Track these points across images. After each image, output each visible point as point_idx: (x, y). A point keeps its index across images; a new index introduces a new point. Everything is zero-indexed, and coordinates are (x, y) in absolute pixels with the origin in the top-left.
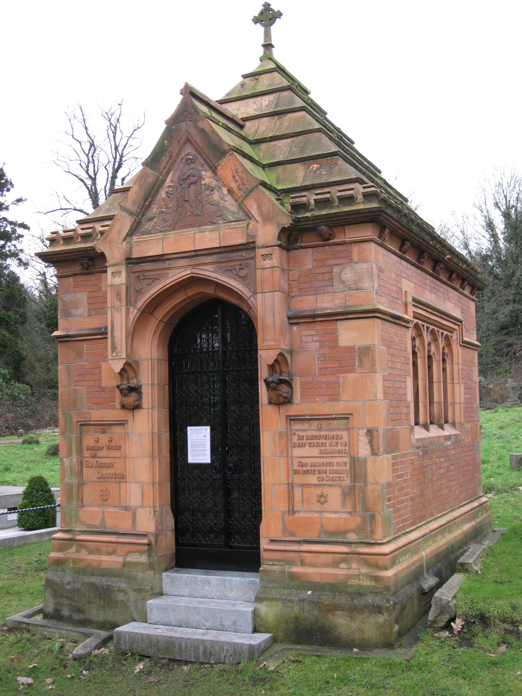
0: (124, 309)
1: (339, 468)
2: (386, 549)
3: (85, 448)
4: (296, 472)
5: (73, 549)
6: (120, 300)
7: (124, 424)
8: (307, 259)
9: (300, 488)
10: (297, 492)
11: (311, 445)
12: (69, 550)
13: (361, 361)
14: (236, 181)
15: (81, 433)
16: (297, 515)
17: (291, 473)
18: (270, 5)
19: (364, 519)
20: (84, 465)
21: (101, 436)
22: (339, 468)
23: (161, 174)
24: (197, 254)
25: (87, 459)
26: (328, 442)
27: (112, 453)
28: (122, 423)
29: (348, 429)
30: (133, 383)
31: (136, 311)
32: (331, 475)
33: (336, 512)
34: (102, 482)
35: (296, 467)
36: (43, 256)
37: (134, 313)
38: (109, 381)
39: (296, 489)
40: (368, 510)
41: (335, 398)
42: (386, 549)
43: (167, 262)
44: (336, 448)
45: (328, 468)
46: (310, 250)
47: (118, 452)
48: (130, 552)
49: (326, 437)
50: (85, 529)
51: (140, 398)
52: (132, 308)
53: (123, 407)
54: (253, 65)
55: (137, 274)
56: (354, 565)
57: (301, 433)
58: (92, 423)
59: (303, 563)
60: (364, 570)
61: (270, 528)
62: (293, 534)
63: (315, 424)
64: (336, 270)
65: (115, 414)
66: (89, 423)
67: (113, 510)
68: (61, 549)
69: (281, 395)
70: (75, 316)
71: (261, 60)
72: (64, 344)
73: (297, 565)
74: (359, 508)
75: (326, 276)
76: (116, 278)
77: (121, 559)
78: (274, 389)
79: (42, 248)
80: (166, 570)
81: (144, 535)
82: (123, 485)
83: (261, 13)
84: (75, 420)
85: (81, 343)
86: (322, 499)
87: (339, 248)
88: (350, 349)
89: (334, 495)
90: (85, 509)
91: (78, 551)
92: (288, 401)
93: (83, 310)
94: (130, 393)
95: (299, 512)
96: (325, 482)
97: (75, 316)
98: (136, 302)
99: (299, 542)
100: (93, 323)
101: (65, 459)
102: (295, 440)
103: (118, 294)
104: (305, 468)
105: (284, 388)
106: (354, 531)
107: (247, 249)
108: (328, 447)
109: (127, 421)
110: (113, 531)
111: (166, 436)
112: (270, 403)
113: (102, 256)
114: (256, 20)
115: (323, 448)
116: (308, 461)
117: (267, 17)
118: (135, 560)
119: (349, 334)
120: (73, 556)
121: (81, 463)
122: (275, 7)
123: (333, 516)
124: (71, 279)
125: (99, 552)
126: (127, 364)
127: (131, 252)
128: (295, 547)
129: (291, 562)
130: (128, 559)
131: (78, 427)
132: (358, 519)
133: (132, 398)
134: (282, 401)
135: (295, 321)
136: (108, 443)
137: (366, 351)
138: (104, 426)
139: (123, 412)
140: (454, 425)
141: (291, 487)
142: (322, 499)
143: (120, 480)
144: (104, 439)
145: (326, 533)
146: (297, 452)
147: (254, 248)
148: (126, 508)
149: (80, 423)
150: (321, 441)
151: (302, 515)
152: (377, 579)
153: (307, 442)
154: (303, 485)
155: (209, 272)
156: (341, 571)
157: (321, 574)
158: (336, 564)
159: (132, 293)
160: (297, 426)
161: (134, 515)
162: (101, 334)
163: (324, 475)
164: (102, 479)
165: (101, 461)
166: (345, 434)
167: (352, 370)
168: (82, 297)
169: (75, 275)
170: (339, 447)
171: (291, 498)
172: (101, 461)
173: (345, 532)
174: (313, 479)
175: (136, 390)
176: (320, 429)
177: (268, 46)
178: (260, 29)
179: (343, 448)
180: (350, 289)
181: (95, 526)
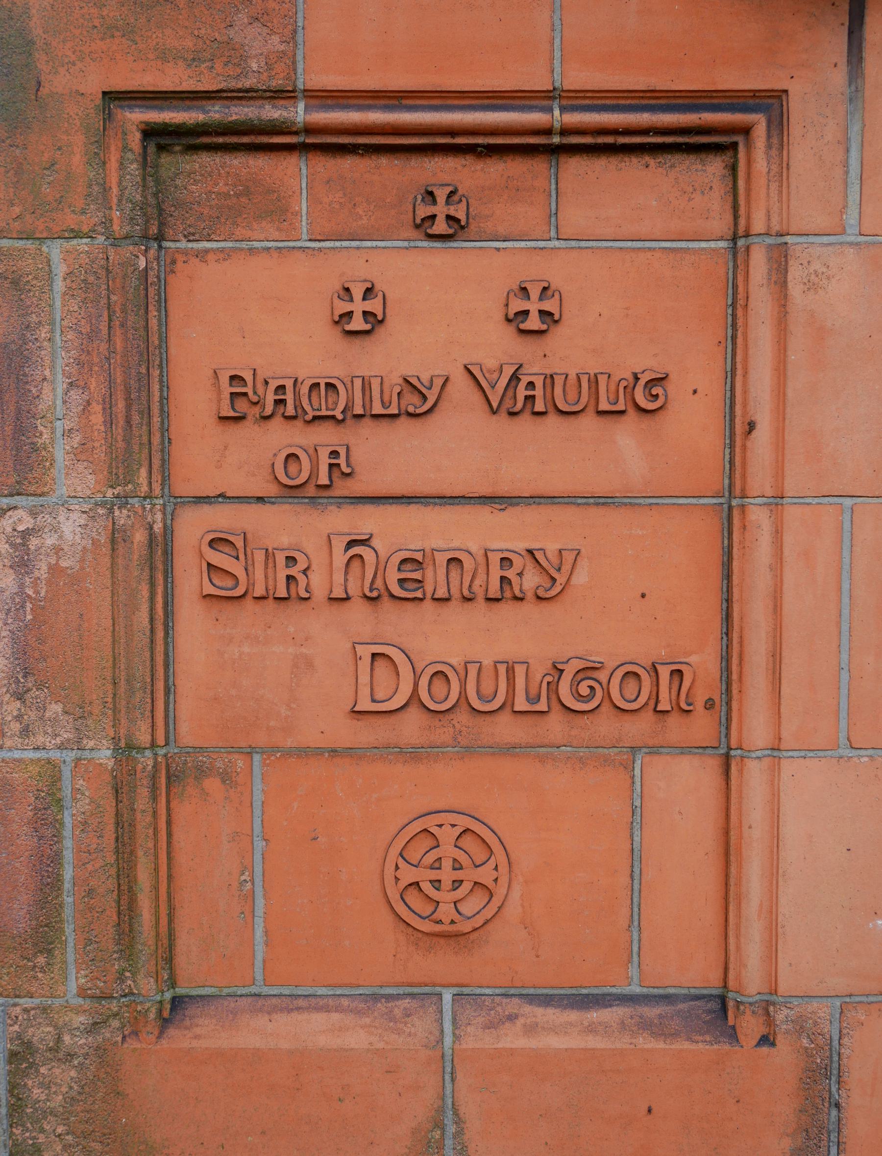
3: (195, 401)
20: (189, 581)
21: (406, 270)
25: (222, 518)
34: (413, 755)
47: (627, 440)
58: (300, 113)
66: (271, 112)
67: (562, 1034)
84: (78, 77)
90: (203, 1034)
109: (772, 103)
121: (161, 550)
131: (123, 171)
136: (496, 348)
143: (638, 728)
144: (445, 309)
149: (136, 117)
165: (395, 532)
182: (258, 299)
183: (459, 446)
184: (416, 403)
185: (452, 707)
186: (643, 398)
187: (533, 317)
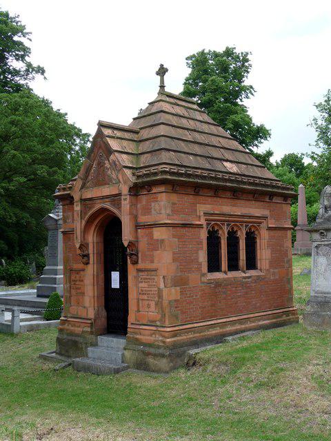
2: (168, 329)
19: (162, 317)
37: (84, 222)
41: (152, 262)
42: (168, 329)
49: (149, 279)
51: (89, 260)
54: (154, 96)
61: (131, 318)
62: (138, 321)
63: (146, 273)
65: (81, 266)
80: (101, 335)
83: (159, 70)
88: (158, 240)
89: (153, 304)
111: (102, 276)
119: (158, 234)
122: (165, 66)
125: (74, 326)
128: (138, 327)
129: (136, 333)
134: (135, 263)
137: (163, 241)
140: (261, 270)
141: (138, 300)
142: (149, 306)
145: (149, 321)
146: (141, 285)
152: (164, 342)
154: (142, 300)
155: (108, 206)
156: (152, 339)
158: (151, 335)
159: (83, 213)
160: (140, 274)
161: (87, 310)
171: (138, 305)
175: (87, 256)
177: (162, 87)
178: (159, 77)
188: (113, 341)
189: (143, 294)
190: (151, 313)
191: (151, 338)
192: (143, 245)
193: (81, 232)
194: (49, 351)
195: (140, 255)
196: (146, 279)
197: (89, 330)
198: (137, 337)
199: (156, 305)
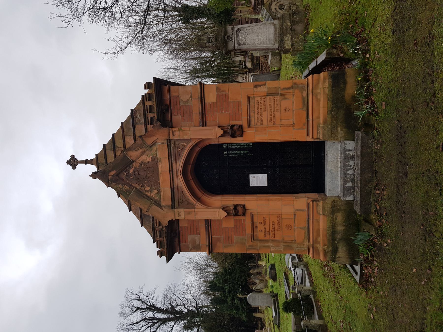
0: (196, 210)
1: (272, 101)
3: (265, 238)
4: (274, 123)
5: (318, 246)
6: (192, 212)
7: (253, 215)
8: (177, 118)
9: (282, 121)
10: (284, 122)
11: (261, 116)
12: (319, 248)
13: (223, 91)
14: (138, 149)
15: (258, 240)
16: (295, 122)
17: (274, 125)
18: (68, 161)
20: (274, 239)
22: (272, 101)
23: (133, 189)
24: (171, 170)
26: (260, 107)
27: (267, 222)
28: (252, 216)
29: (254, 97)
30: (232, 208)
31: (197, 204)
32: (276, 105)
33: (293, 103)
35: (272, 123)
36: (168, 260)
37: (198, 205)
38: (230, 223)
39: (282, 123)
40: (292, 86)
43: (175, 186)
44: (263, 103)
45: (272, 107)
46: (173, 117)
48: (317, 212)
49: (258, 108)
50: (307, 239)
52: (196, 206)
53: (244, 214)
55: (180, 203)
56: (318, 91)
57: (256, 121)
59: (319, 117)
60: (321, 85)
63: (251, 114)
64: (182, 104)
65: (247, 219)
67: (296, 222)
68: (319, 254)
69: (238, 129)
70: (199, 242)
71: (92, 164)
72: (213, 249)
73: (320, 120)
74: (291, 91)
75: (184, 107)
76: (181, 214)
77: (322, 217)
78: (235, 132)
79: (164, 258)
80: (326, 196)
81: (308, 204)
82: (283, 216)
83: (71, 165)
84: (251, 243)
85: (213, 239)
86: (287, 110)
87: (172, 101)
88: (218, 96)
89: (285, 104)
90: (296, 239)
91: (319, 243)
92: (241, 127)
93: (197, 237)
94: (238, 211)
95: (293, 121)
96: (279, 109)
97: (199, 242)
98: (193, 204)
99: (308, 121)
100: (203, 230)
101: (271, 250)
102: (259, 124)
103: (189, 213)
104: (273, 119)
105: (235, 128)
106: (302, 93)
107: (170, 144)
108: (263, 107)
109: (251, 213)
110: (307, 222)
112: (242, 136)
113: (171, 222)
114: (74, 168)
115: (263, 110)
116: (269, 117)
117: (73, 162)
118: (321, 209)
120: (322, 245)
121: (272, 240)
123: (295, 104)
124: (181, 244)
125: (318, 230)
126: (223, 209)
127: (168, 206)
130: (321, 213)
131: (255, 241)
132: (296, 91)
133: (240, 209)
135: (204, 123)
136: (262, 225)
138: (254, 227)
139: (246, 215)
141: (281, 126)
142: (287, 110)
144: (260, 227)
145: (303, 108)
146: (265, 122)
147: (170, 140)
148: (295, 215)
150: (260, 111)
151: (295, 120)
153: (260, 118)
154: (281, 120)
155: (179, 164)
157: (323, 107)
158: (318, 100)
159: (188, 205)
160: (253, 123)
161: (298, 210)
162: (208, 222)
163: (276, 109)
164: (280, 227)
165: (271, 229)
166: (256, 99)
167: (227, 95)
168: (190, 237)
169: (179, 241)
170: (263, 102)
171: (287, 126)
172: (271, 229)
173: (303, 98)
174: (277, 114)
175: (236, 207)
176: (254, 112)
179: (263, 100)
180: (191, 97)
181: (305, 233)
182: (261, 236)
183: (267, 227)
184: (265, 228)
185: (280, 227)
186: (264, 218)
187: (261, 223)
188: (330, 171)
189: (274, 117)
190: (295, 106)
191: (322, 99)
192: (225, 119)
193: (208, 208)
194: (354, 274)
195: (233, 123)
196: (258, 113)
197: (320, 203)
198: (321, 121)
199: (286, 98)
